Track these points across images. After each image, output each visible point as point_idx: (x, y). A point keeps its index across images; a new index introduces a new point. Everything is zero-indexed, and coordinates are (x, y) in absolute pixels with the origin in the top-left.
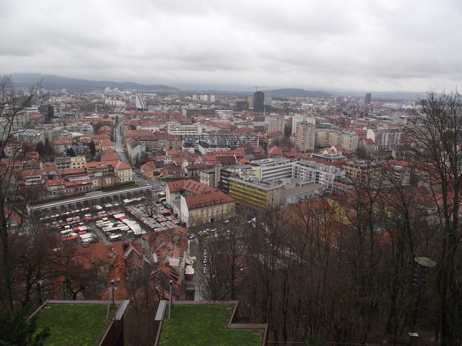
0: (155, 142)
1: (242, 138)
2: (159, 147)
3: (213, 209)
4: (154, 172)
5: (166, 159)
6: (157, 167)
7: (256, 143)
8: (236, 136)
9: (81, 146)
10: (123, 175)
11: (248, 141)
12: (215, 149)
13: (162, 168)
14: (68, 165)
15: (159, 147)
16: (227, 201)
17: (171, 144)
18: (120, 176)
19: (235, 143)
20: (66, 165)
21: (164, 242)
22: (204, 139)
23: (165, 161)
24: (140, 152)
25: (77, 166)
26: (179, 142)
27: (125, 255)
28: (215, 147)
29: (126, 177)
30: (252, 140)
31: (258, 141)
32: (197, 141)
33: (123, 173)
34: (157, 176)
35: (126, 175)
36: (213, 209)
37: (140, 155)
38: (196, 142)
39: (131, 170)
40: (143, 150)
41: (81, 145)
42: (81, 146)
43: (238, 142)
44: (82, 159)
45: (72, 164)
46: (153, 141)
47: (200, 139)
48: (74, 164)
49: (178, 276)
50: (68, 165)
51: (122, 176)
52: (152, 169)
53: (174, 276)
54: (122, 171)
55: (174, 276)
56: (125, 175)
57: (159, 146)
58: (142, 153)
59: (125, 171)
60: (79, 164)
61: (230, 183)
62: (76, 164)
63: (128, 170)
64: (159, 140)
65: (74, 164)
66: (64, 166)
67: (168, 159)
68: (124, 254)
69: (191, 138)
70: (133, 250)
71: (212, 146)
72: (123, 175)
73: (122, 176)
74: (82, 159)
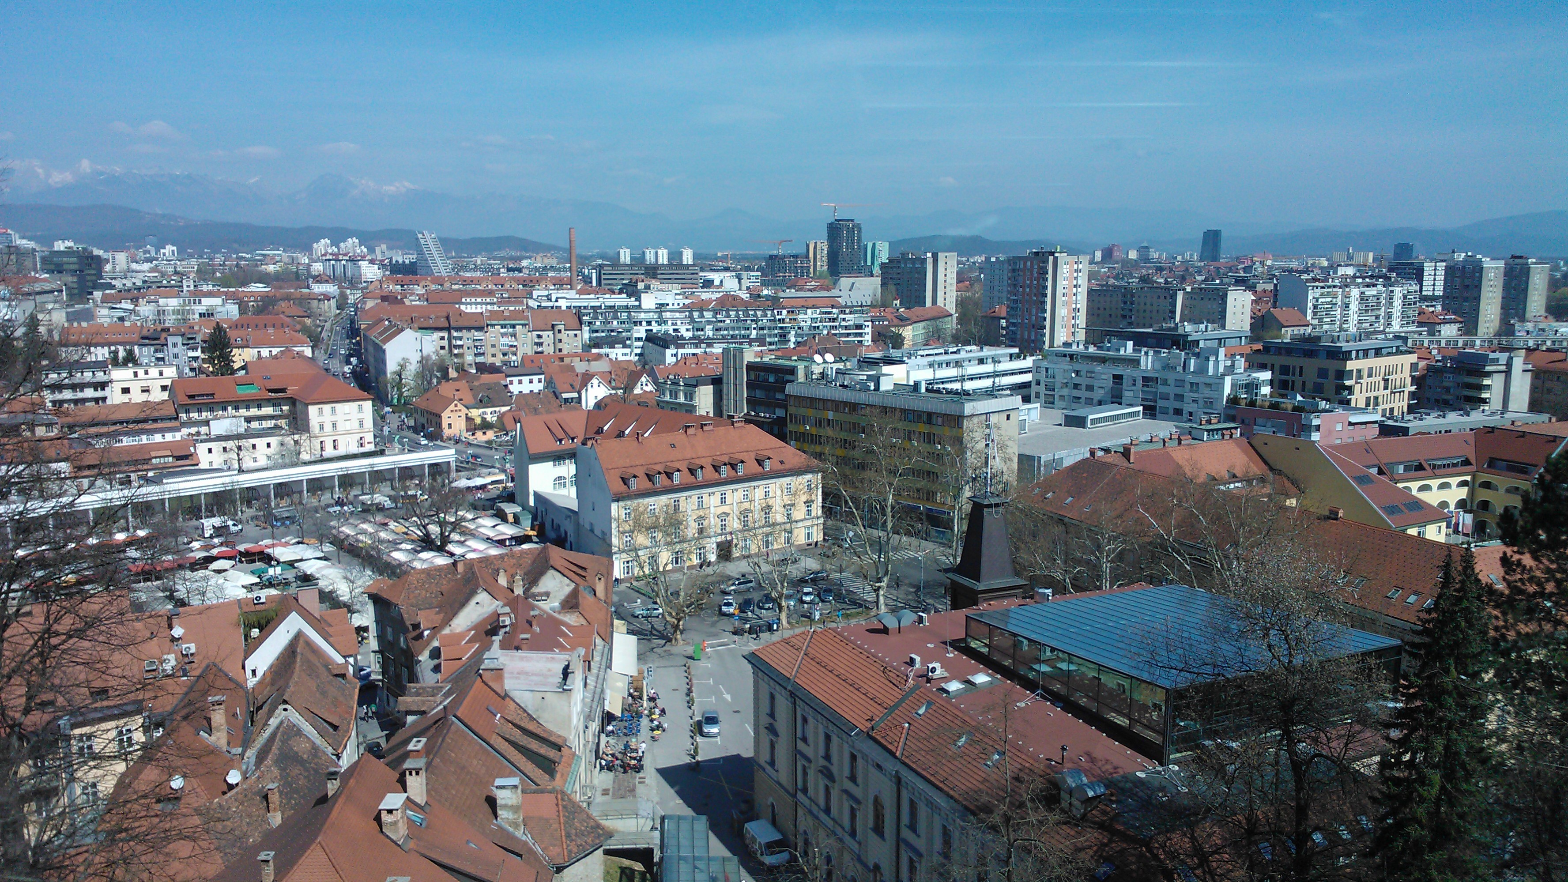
0: (478, 335)
1: (806, 318)
2: (494, 355)
3: (723, 501)
4: (469, 419)
5: (520, 382)
6: (482, 403)
7: (861, 335)
8: (785, 312)
9: (176, 350)
10: (334, 425)
11: (833, 327)
12: (708, 350)
13: (504, 409)
14: (99, 394)
15: (494, 355)
16: (787, 466)
17: (540, 344)
18: (322, 427)
19: (783, 337)
20: (89, 393)
21: (482, 597)
22: (665, 322)
23: (515, 388)
24: (415, 358)
25: (137, 397)
26: (572, 333)
27: (250, 664)
28: (710, 345)
29: (348, 433)
30: (843, 323)
31: (868, 330)
32: (640, 332)
33: (334, 418)
34: (479, 434)
35: (348, 426)
36: (723, 501)
37: (413, 368)
38: (636, 335)
39: (368, 405)
40: (425, 353)
41: (175, 345)
42: (176, 350)
43: (793, 333)
44: (161, 374)
45: (117, 387)
46: (469, 329)
47: (649, 323)
48: (126, 391)
49: (559, 748)
50: (99, 394)
51: (328, 428)
52: (460, 407)
53: (534, 745)
54: (327, 408)
55: (534, 745)
56: (340, 427)
57: (493, 350)
58: (424, 361)
59: (338, 406)
60: (146, 390)
61: (792, 410)
62: (135, 388)
63: (354, 405)
64: (493, 326)
65: (126, 391)
66: (80, 395)
67: (526, 379)
68: (246, 658)
69: (616, 318)
70: (299, 635)
71: (697, 341)
72: (334, 425)
73: (328, 428)
74: (161, 374)
